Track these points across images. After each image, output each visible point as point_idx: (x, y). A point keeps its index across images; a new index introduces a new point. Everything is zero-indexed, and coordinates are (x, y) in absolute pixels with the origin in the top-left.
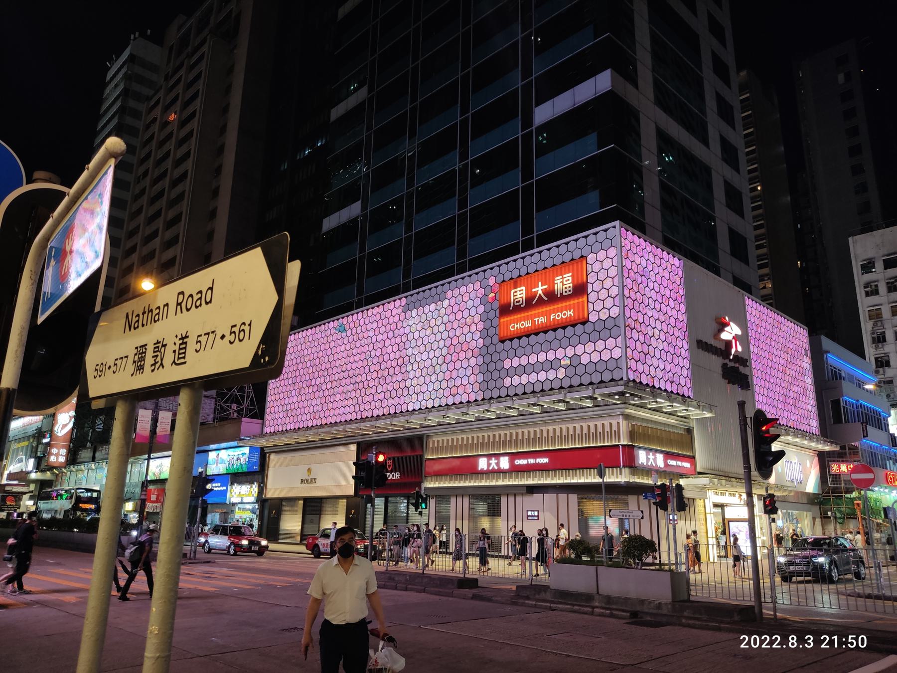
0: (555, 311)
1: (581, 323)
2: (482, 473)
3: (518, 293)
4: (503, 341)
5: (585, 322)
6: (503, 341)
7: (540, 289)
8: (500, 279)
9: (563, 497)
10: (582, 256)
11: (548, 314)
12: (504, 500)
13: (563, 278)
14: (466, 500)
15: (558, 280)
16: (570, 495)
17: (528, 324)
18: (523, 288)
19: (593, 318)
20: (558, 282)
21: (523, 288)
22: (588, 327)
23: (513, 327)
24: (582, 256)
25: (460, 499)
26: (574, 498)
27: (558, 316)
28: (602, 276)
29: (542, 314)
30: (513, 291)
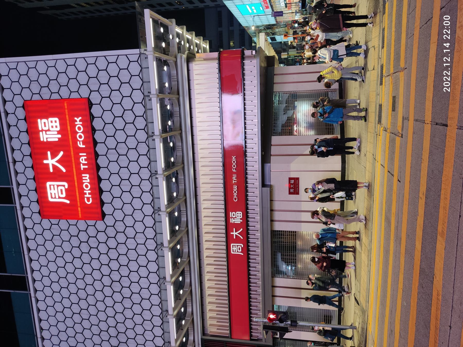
0: (75, 141)
1: (90, 108)
2: (247, 249)
3: (53, 191)
4: (103, 215)
5: (91, 105)
6: (103, 215)
7: (51, 162)
8: (37, 218)
9: (274, 150)
10: (23, 107)
11: (78, 150)
12: (278, 227)
13: (42, 131)
14: (279, 281)
15: (43, 137)
16: (272, 153)
17: (86, 178)
18: (48, 184)
19: (84, 93)
20: (45, 136)
21: (48, 184)
22: (95, 98)
23: (88, 199)
24: (23, 107)
25: (278, 292)
26: (275, 140)
27: (80, 137)
28: (44, 80)
29: (77, 158)
30: (51, 200)
